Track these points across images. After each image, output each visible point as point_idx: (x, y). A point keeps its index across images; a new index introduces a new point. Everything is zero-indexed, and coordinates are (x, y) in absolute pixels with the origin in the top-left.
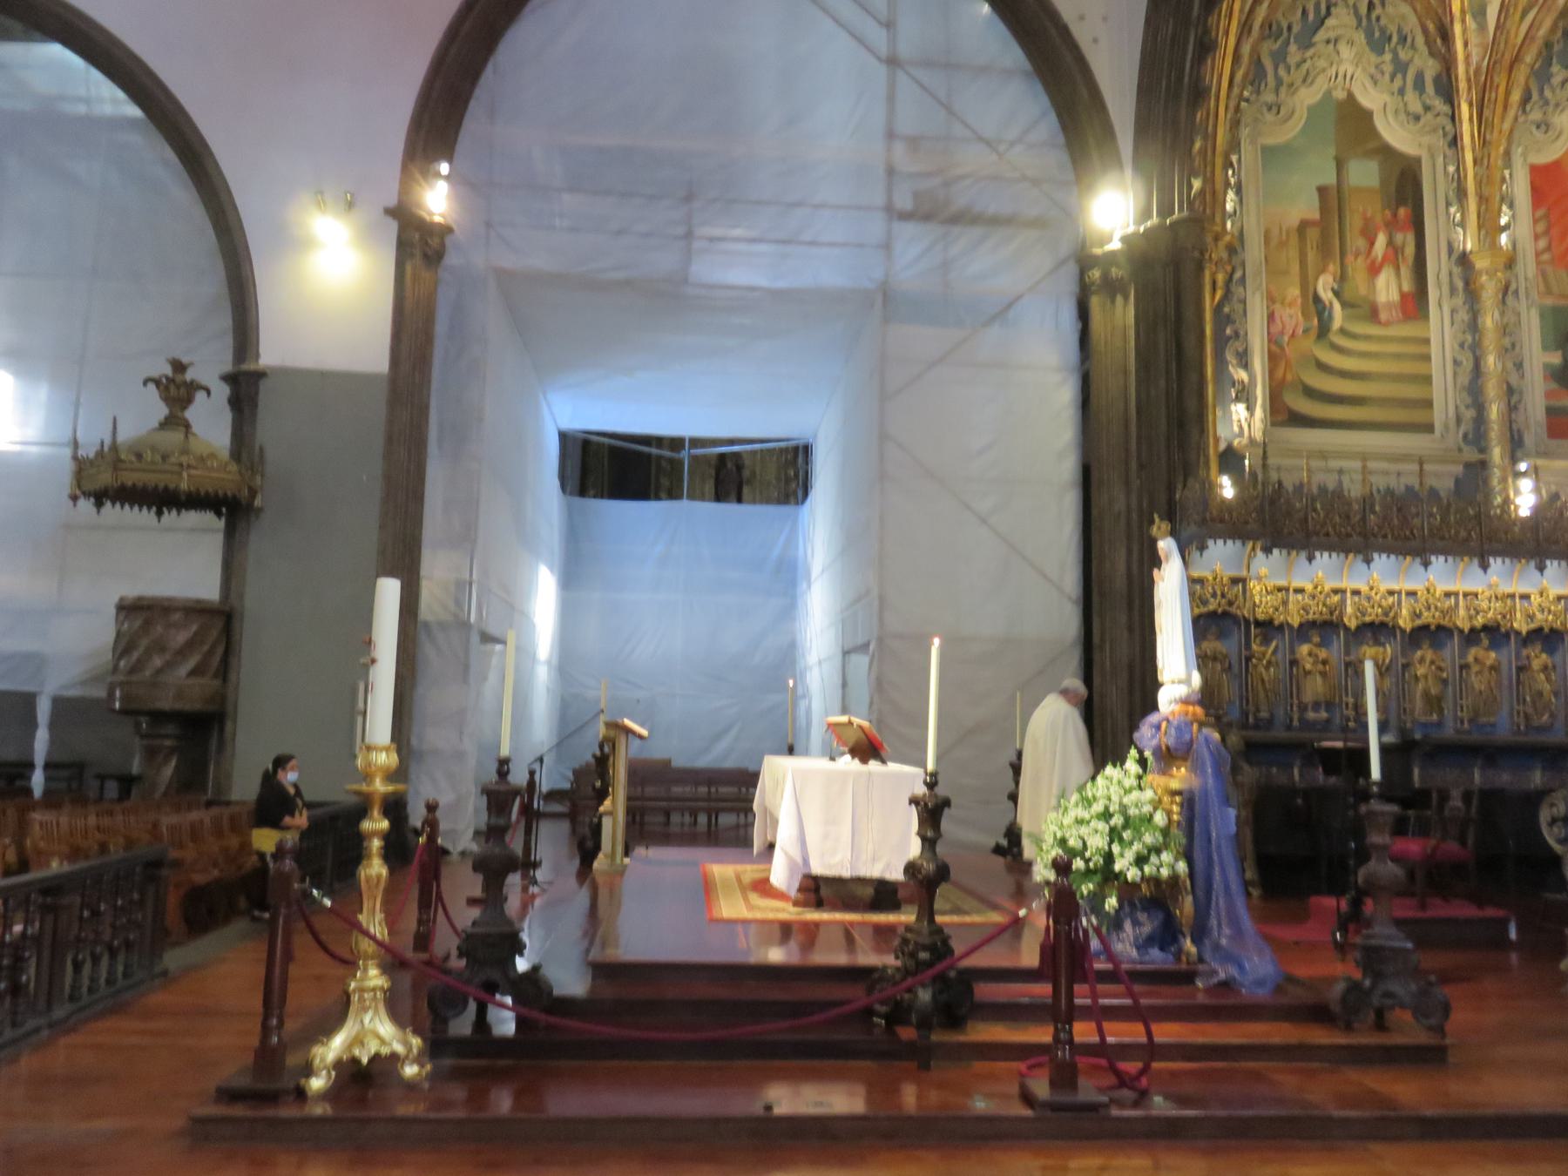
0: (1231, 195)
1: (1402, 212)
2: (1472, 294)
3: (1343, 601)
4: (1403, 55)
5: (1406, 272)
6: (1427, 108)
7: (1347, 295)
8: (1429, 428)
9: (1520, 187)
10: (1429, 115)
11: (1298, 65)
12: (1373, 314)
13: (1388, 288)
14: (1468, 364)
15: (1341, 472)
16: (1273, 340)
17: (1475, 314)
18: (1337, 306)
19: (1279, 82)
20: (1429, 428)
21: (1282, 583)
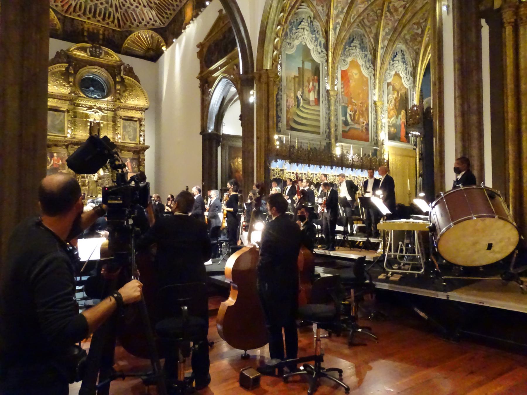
0: (279, 66)
1: (316, 77)
2: (329, 101)
3: (302, 176)
4: (317, 36)
5: (316, 93)
6: (322, 51)
7: (304, 97)
8: (319, 133)
9: (339, 76)
11: (295, 33)
13: (312, 97)
14: (327, 118)
15: (301, 143)
17: (329, 106)
18: (302, 100)
19: (291, 37)
21: (289, 171)
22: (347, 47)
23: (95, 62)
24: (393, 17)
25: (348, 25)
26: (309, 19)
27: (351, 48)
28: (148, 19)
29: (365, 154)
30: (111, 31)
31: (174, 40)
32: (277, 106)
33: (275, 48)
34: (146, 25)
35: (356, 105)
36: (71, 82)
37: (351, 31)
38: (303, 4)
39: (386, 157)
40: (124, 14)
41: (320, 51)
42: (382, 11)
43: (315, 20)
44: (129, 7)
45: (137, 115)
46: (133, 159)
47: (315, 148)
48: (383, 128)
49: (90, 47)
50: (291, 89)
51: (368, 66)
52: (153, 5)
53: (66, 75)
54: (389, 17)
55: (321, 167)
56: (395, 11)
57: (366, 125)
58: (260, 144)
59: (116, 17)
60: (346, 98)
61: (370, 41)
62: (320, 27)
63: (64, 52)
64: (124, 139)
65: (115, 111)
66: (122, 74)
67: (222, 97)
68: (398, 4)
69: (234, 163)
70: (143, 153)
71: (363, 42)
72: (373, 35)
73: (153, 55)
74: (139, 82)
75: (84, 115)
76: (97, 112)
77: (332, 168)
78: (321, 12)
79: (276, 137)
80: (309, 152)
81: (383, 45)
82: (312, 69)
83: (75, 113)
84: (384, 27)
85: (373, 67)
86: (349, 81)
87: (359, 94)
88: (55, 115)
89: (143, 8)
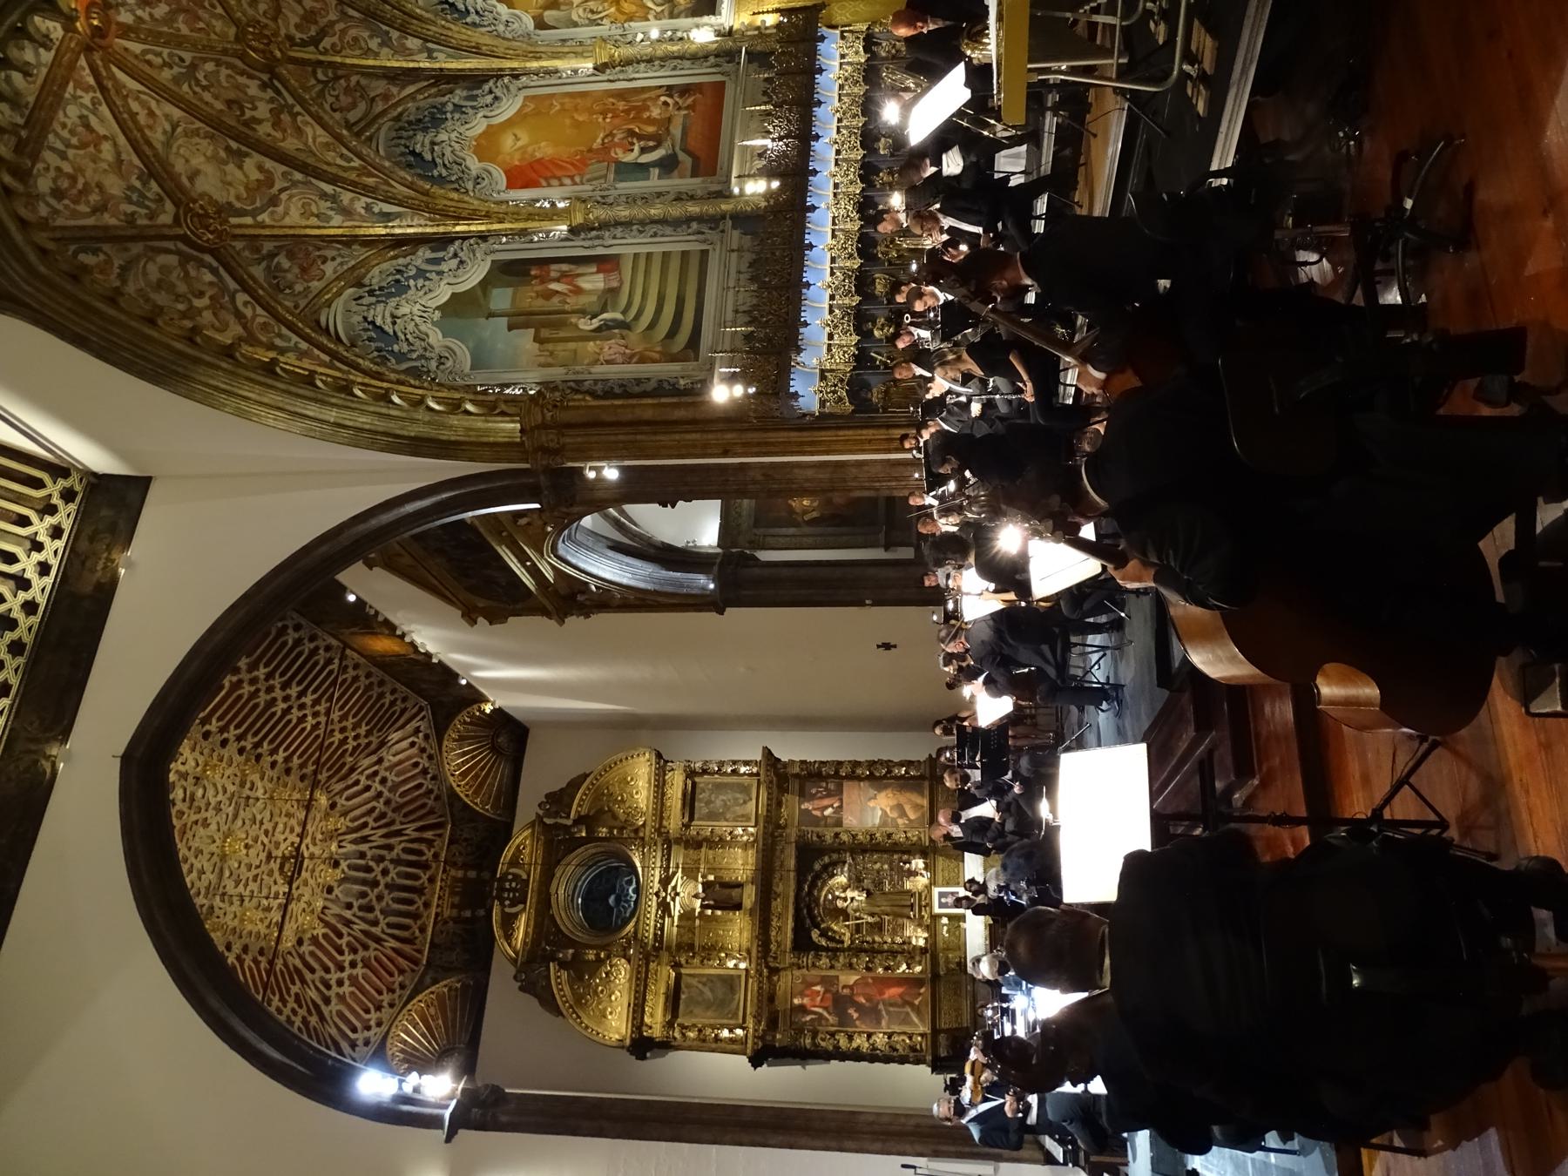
2: (604, 225)
3: (839, 307)
5: (580, 270)
6: (455, 255)
7: (596, 309)
8: (704, 253)
10: (461, 254)
11: (410, 344)
12: (613, 292)
13: (593, 282)
15: (736, 312)
16: (629, 359)
17: (617, 224)
18: (605, 316)
19: (421, 357)
20: (704, 253)
22: (436, 173)
23: (540, 893)
24: (332, 24)
25: (371, 175)
26: (364, 301)
27: (438, 161)
28: (414, 750)
29: (765, 93)
30: (453, 847)
31: (464, 682)
32: (627, 395)
33: (455, 407)
34: (430, 757)
35: (611, 134)
36: (598, 955)
37: (387, 164)
38: (323, 323)
39: (771, 20)
40: (405, 815)
41: (455, 262)
42: (320, 63)
43: (366, 281)
44: (388, 802)
45: (676, 784)
46: (803, 795)
47: (751, 265)
48: (679, 34)
49: (502, 905)
50: (575, 351)
51: (489, 99)
52: (374, 739)
53: (583, 971)
54: (335, 39)
55: (811, 247)
56: (316, 23)
57: (671, 96)
58: (744, 444)
59: (416, 835)
60: (596, 168)
61: (412, 97)
62: (385, 266)
63: (518, 971)
64: (746, 817)
65: (669, 843)
66: (569, 822)
67: (611, 553)
68: (293, 11)
69: (805, 512)
70: (785, 765)
71: (419, 121)
72: (394, 90)
73: (508, 735)
74: (586, 776)
75: (684, 923)
76: (674, 888)
77: (813, 208)
78: (341, 264)
79: (723, 394)
80: (764, 286)
81: (420, 51)
82: (509, 285)
83: (679, 947)
84: (368, 52)
85: (491, 83)
86: (539, 161)
87: (577, 125)
88: (690, 999)
89: (386, 764)
